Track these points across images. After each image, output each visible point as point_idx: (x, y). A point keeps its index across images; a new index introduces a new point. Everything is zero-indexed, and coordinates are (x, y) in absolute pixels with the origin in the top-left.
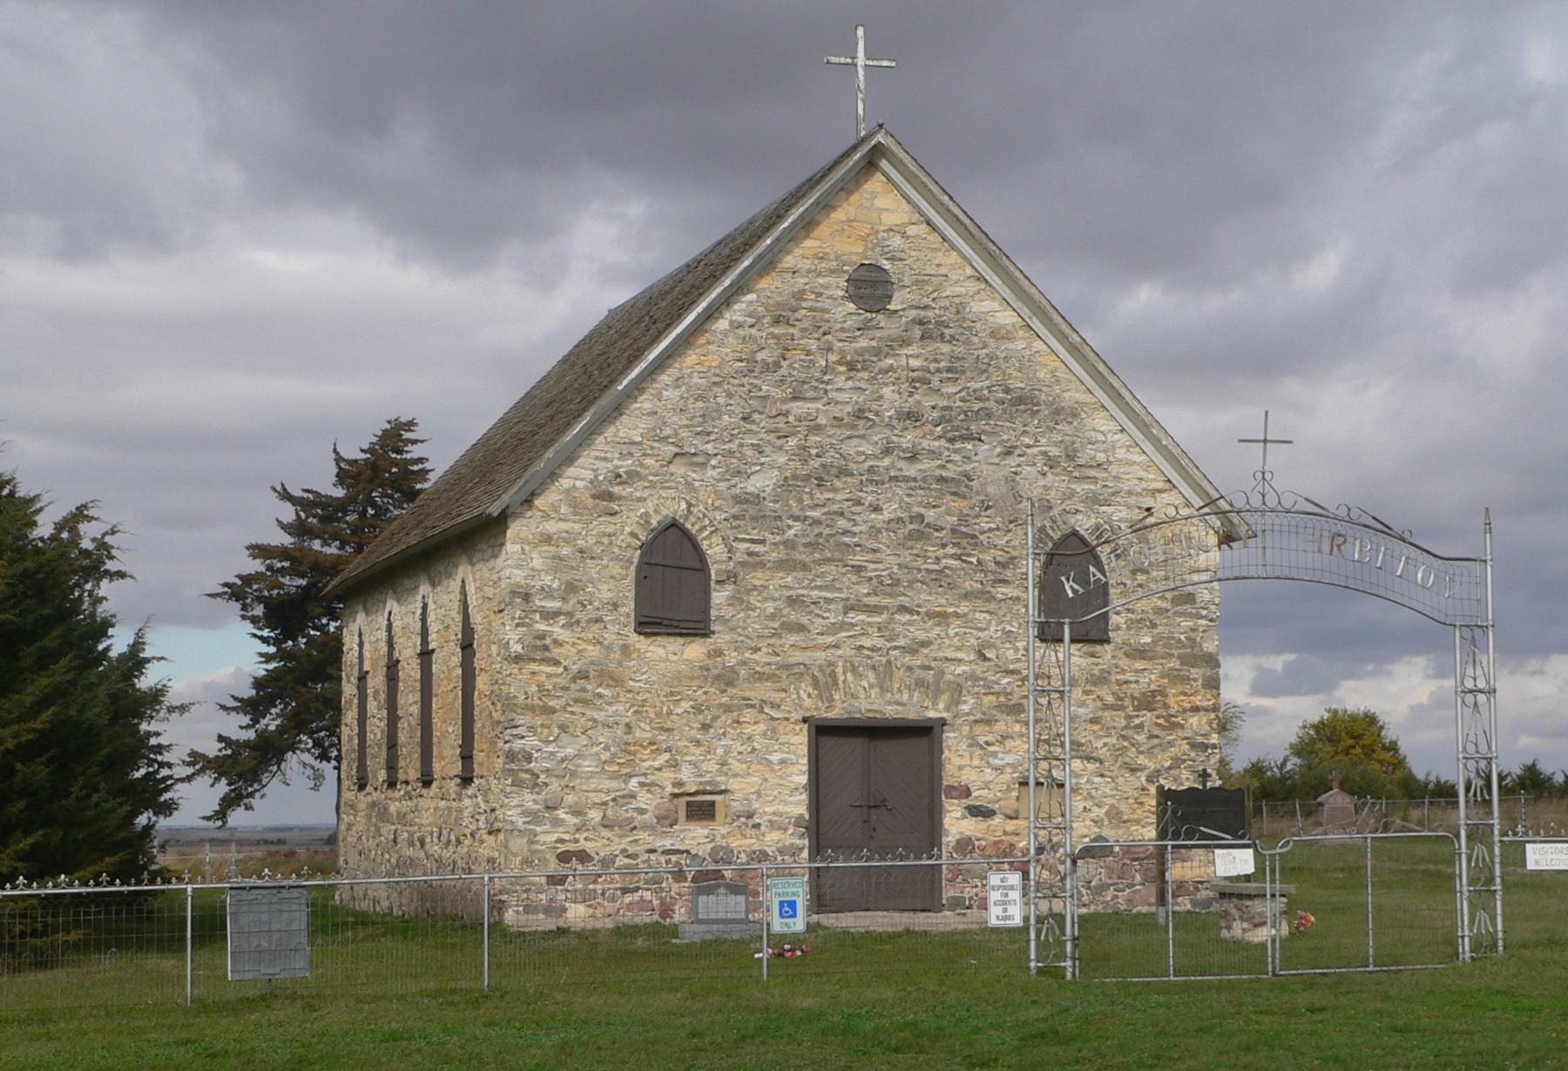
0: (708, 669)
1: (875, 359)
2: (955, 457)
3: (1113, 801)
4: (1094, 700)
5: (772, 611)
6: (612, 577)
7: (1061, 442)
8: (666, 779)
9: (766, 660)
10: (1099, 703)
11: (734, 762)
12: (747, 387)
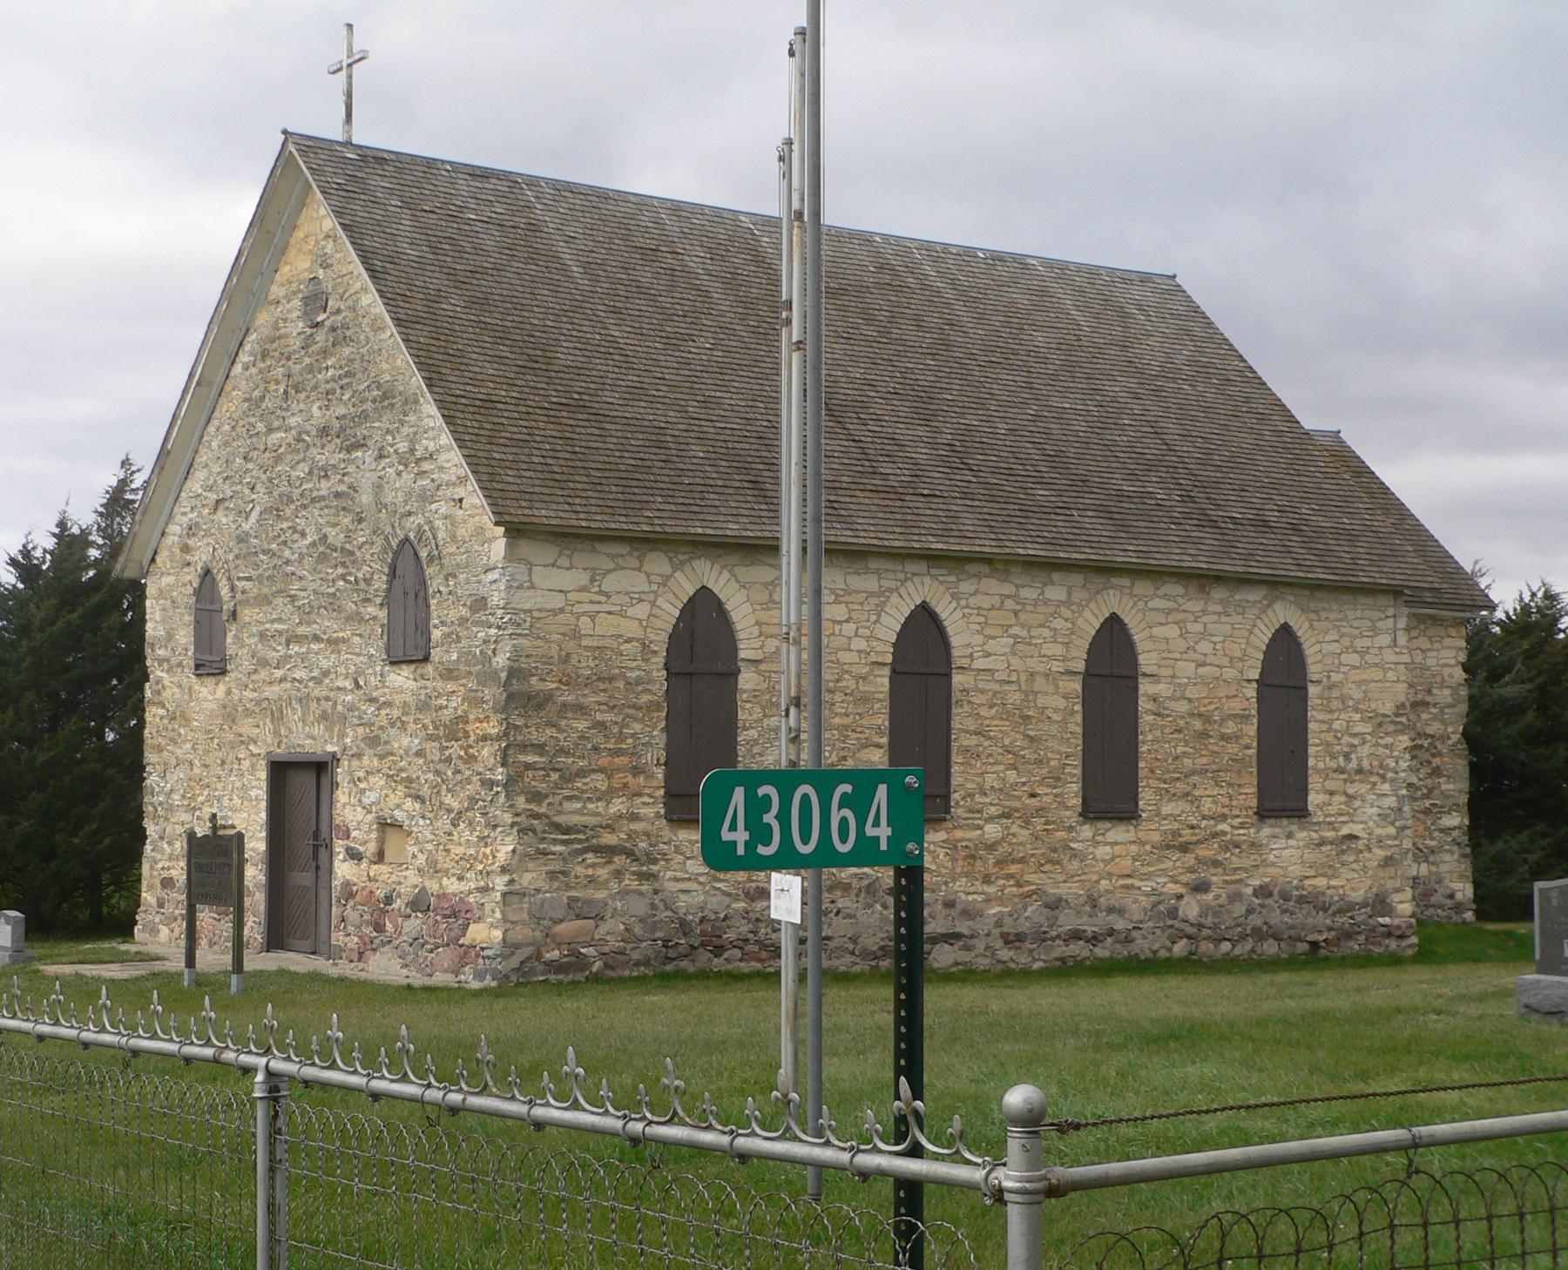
1: (310, 376)
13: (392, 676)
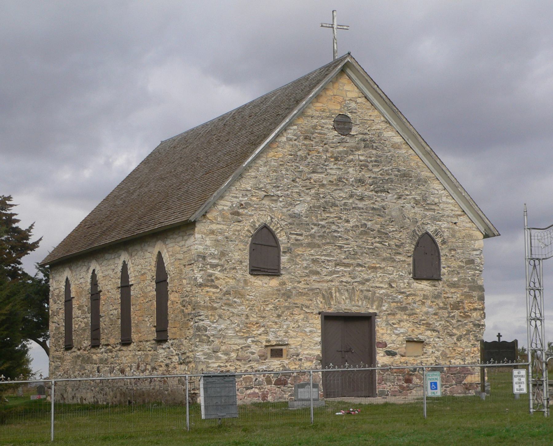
0: (280, 291)
1: (346, 156)
2: (379, 199)
3: (444, 349)
4: (435, 305)
5: (306, 265)
6: (240, 249)
7: (421, 193)
8: (263, 339)
9: (303, 287)
10: (437, 306)
11: (291, 332)
12: (294, 167)
13: (415, 284)
